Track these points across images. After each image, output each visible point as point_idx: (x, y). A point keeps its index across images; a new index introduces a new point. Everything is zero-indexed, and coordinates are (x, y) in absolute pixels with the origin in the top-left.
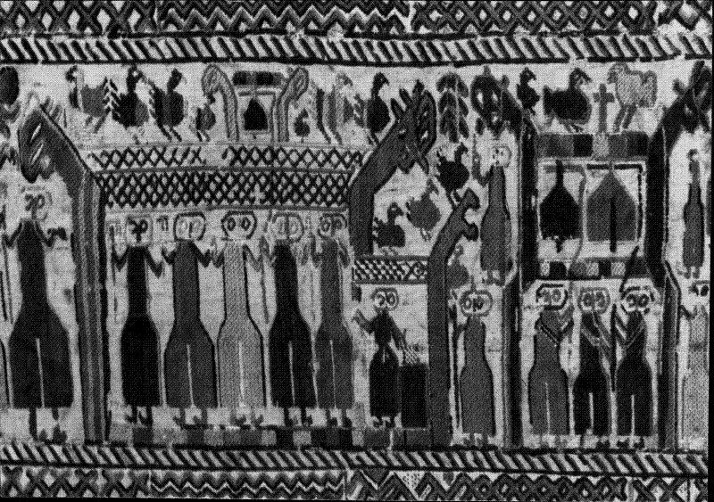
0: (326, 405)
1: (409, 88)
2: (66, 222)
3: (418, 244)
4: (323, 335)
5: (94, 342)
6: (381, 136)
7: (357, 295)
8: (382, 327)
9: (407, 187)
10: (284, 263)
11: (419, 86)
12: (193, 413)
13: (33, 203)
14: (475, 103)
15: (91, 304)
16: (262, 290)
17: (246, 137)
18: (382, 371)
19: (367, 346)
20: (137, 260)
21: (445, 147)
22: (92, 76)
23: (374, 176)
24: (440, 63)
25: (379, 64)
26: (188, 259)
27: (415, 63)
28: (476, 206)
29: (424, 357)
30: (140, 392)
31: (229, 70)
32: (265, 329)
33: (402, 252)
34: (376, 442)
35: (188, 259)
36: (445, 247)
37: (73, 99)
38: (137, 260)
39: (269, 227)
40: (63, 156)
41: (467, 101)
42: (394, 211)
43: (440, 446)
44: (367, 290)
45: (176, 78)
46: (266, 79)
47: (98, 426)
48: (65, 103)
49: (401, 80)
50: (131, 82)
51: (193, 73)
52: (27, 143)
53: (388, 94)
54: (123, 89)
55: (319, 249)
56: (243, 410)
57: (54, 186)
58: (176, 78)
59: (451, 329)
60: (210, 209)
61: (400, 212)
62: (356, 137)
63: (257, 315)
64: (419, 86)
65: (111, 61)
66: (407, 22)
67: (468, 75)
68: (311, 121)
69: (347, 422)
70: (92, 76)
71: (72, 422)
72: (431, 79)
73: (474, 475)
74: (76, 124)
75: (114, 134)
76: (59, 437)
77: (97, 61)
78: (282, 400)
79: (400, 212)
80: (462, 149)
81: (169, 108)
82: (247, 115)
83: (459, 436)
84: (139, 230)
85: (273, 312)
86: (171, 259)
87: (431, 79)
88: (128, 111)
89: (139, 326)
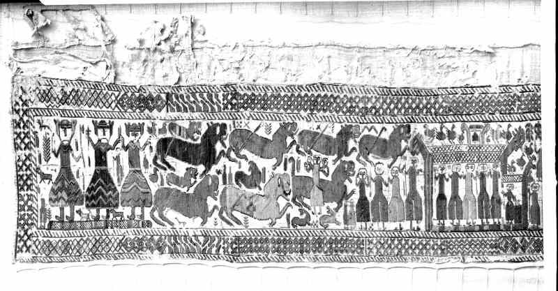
0: (493, 218)
1: (517, 128)
2: (422, 167)
3: (520, 171)
4: (493, 198)
5: (429, 201)
6: (509, 142)
7: (503, 186)
8: (509, 195)
9: (516, 155)
10: (482, 177)
11: (520, 127)
12: (456, 221)
13: (414, 162)
14: (535, 132)
15: (428, 192)
16: (476, 185)
17: (472, 143)
18: (508, 207)
19: (505, 200)
20: (442, 177)
21: (527, 144)
22: (431, 126)
23: (506, 154)
24: (526, 120)
25: (509, 121)
26: (455, 177)
27: (519, 121)
28: (535, 159)
29: (521, 203)
30: (441, 216)
31: (468, 124)
32: (477, 197)
33: (515, 173)
34: (507, 228)
35: (455, 177)
36: (527, 172)
37: (425, 133)
38: (442, 178)
39: (478, 168)
40: (422, 148)
41: (533, 130)
42: (513, 162)
43: (525, 229)
44: (505, 184)
45: (453, 127)
46: (478, 127)
47: (429, 227)
48: (423, 134)
49: (515, 125)
50: (441, 128)
51: (458, 125)
52: (413, 145)
53: (511, 130)
54: (439, 130)
55: (492, 173)
56: (470, 220)
57: (420, 157)
58: (453, 127)
59: (528, 194)
60: (462, 163)
61: (514, 162)
62: (503, 142)
63: (475, 193)
64: (520, 127)
65: (436, 122)
66: (515, 109)
67: (533, 123)
68: (491, 138)
69: (499, 223)
70: (431, 126)
71: (422, 225)
72: (523, 125)
73: (536, 238)
74: (425, 139)
75: (437, 143)
76: (419, 229)
77: (432, 122)
78: (481, 217)
79: (514, 162)
80: (532, 144)
81: (451, 135)
82: (473, 137)
83: (530, 225)
84: (442, 169)
85: (479, 192)
86: (451, 177)
87: (523, 125)
88: (441, 136)
89: (442, 197)
